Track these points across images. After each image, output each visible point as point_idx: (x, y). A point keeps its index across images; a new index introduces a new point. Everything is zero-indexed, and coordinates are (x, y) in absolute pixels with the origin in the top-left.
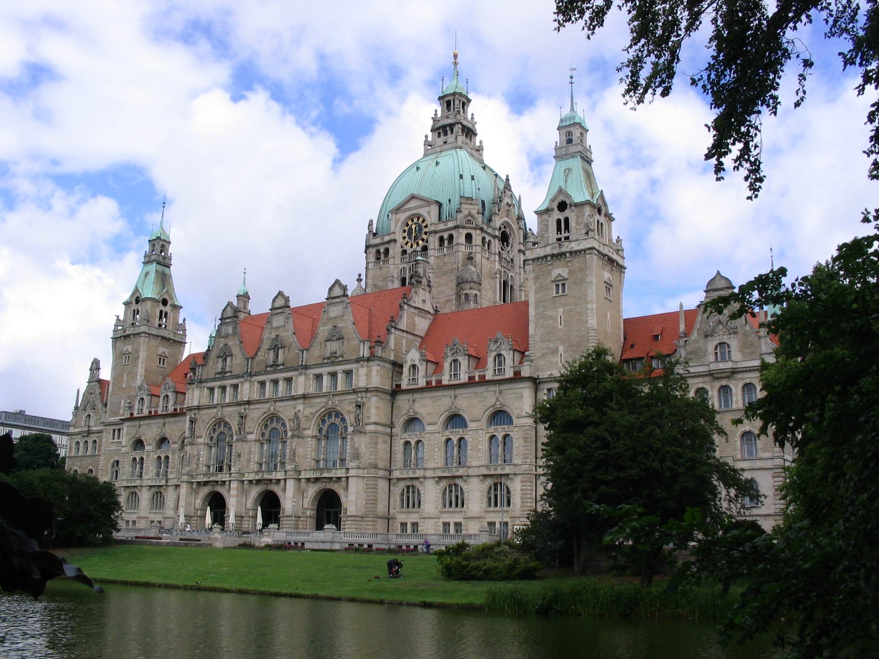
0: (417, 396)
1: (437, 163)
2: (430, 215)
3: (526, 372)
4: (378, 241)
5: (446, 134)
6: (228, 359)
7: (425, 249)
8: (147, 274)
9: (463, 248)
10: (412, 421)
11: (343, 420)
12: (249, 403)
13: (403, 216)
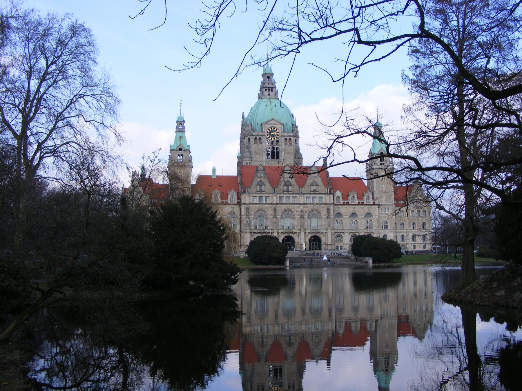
0: (340, 206)
1: (276, 106)
2: (280, 129)
3: (377, 203)
4: (256, 134)
5: (269, 90)
6: (263, 186)
7: (278, 141)
8: (181, 137)
9: (295, 144)
10: (339, 215)
11: (319, 213)
12: (277, 204)
13: (268, 126)
